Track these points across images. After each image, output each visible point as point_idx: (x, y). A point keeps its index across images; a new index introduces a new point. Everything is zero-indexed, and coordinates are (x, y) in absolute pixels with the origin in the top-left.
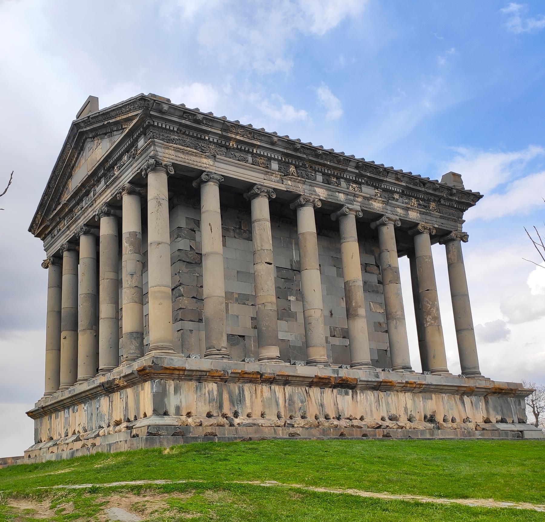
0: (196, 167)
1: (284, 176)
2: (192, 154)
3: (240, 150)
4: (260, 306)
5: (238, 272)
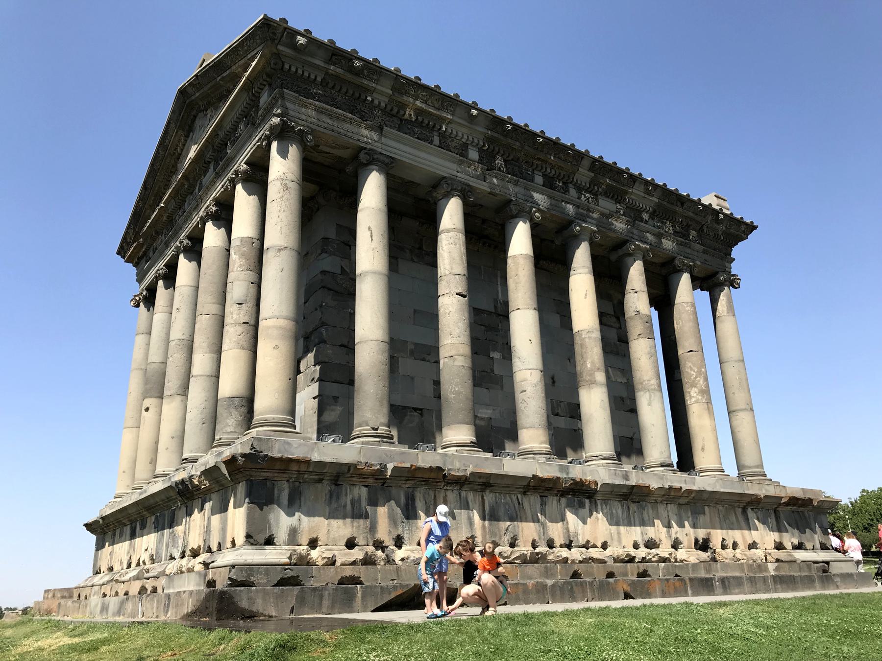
0: (351, 140)
1: (488, 170)
2: (345, 120)
3: (420, 124)
4: (446, 360)
5: (415, 311)
